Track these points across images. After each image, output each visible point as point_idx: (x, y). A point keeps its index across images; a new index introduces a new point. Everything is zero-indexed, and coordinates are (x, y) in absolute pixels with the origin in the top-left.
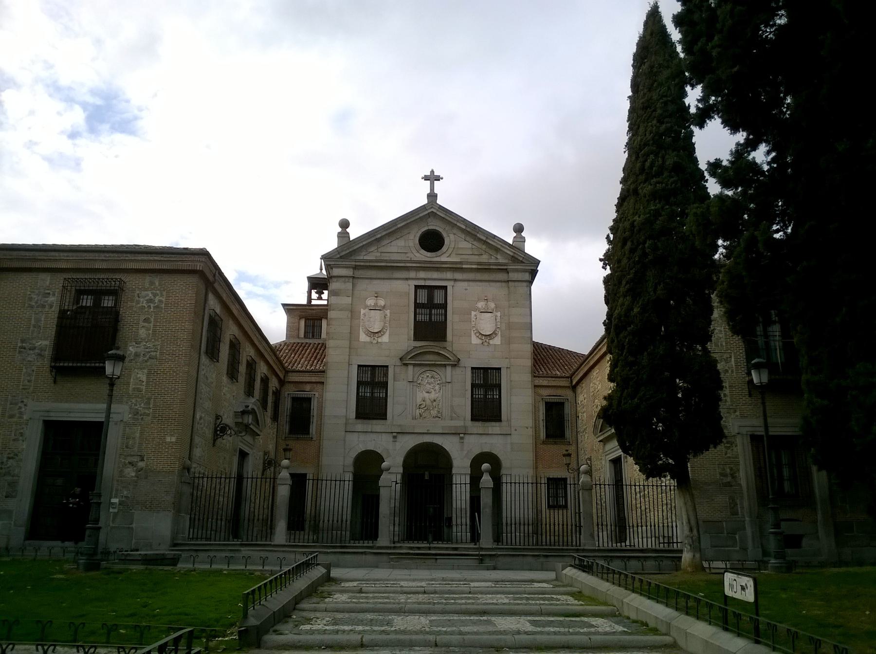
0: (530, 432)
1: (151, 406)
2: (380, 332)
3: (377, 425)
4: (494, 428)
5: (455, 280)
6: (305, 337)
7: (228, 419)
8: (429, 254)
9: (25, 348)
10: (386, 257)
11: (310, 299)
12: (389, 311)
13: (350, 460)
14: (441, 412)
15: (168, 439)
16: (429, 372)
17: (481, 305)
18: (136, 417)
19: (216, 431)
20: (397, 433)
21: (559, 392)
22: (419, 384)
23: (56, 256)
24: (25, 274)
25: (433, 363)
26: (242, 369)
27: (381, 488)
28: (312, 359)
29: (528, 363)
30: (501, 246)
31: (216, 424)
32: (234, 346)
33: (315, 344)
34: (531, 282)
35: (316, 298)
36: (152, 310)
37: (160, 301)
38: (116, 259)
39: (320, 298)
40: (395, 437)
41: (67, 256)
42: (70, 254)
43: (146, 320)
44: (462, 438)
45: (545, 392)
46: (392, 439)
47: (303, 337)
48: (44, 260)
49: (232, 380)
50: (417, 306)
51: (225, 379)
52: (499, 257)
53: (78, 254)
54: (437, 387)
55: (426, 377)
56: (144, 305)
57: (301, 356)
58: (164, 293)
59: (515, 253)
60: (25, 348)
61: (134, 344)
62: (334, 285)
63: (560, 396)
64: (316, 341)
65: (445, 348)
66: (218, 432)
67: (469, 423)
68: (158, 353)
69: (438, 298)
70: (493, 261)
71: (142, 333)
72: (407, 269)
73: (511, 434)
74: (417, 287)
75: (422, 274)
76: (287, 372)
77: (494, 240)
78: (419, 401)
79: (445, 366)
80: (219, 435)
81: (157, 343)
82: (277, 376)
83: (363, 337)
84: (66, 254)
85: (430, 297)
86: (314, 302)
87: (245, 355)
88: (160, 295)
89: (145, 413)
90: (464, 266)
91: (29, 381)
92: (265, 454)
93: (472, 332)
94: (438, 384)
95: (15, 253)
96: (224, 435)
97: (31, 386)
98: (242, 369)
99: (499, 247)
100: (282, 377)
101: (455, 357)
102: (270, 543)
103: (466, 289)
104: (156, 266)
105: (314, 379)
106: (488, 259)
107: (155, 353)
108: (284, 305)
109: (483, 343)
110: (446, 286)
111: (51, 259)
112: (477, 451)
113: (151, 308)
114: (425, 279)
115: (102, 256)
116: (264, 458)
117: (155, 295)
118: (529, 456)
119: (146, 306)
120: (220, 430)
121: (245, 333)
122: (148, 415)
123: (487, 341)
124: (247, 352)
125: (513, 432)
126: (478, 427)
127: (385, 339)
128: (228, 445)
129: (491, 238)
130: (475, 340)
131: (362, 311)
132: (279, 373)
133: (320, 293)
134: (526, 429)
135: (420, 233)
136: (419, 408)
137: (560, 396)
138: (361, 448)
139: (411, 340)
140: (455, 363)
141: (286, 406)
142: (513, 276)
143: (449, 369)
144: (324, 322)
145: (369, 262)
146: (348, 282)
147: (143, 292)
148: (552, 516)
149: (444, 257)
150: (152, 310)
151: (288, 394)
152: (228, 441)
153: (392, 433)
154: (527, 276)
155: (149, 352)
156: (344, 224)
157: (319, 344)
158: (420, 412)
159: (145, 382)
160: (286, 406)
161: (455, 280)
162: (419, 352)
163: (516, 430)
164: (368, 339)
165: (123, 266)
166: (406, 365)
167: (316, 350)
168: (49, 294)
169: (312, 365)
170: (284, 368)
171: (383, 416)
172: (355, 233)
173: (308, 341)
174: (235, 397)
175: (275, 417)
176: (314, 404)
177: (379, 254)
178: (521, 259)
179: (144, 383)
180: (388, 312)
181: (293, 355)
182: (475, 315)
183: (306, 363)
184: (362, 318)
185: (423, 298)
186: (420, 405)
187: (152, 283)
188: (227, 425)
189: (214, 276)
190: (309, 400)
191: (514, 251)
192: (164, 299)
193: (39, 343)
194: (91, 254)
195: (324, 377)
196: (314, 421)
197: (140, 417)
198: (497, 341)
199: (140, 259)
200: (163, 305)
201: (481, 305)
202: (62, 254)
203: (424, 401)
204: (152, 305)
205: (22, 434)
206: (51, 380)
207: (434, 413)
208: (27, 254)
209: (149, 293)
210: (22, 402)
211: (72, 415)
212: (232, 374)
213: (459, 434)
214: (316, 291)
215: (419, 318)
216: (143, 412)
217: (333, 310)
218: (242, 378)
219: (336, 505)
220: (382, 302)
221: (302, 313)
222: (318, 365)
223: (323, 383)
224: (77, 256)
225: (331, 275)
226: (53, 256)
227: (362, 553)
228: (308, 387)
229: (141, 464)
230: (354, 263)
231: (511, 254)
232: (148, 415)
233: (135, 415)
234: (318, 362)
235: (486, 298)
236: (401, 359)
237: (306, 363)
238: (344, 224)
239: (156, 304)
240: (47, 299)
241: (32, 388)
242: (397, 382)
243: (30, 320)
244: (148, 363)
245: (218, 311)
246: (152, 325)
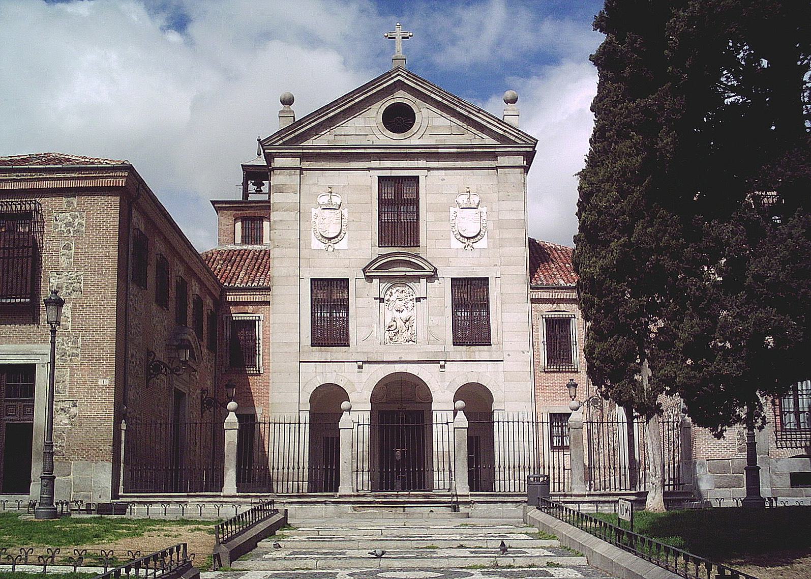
0: (527, 357)
1: (80, 345)
2: (336, 237)
3: (337, 353)
4: (480, 352)
5: (429, 169)
6: (245, 240)
7: (161, 355)
8: (396, 136)
10: (342, 141)
11: (246, 193)
12: (346, 209)
13: (306, 397)
15: (101, 382)
16: (399, 285)
17: (463, 199)
18: (64, 358)
19: (148, 369)
20: (364, 362)
21: (563, 306)
25: (404, 274)
26: (172, 293)
27: (341, 430)
28: (254, 273)
29: (523, 269)
30: (488, 122)
31: (148, 361)
32: (163, 268)
33: (256, 251)
34: (526, 169)
35: (254, 191)
36: (72, 234)
37: (80, 224)
39: (259, 192)
40: (360, 367)
43: (65, 247)
44: (443, 367)
45: (545, 307)
46: (357, 370)
47: (240, 242)
49: (162, 308)
50: (381, 202)
51: (154, 307)
52: (484, 136)
54: (410, 304)
56: (62, 229)
57: (239, 268)
58: (84, 215)
59: (505, 131)
61: (55, 275)
62: (277, 179)
63: (564, 311)
64: (257, 247)
65: (417, 256)
66: (152, 371)
67: (451, 347)
68: (82, 284)
69: (408, 194)
70: (477, 142)
71: (64, 262)
72: (368, 157)
73: (503, 361)
74: (380, 179)
75: (388, 163)
76: (225, 291)
77: (479, 115)
78: (388, 321)
79: (417, 278)
80: (152, 374)
81: (79, 273)
82: (211, 294)
83: (317, 244)
85: (399, 193)
86: (251, 198)
87: (173, 274)
88: (79, 217)
89: (73, 353)
90: (440, 150)
92: (203, 392)
93: (451, 232)
94: (411, 300)
96: (158, 374)
98: (172, 293)
99: (485, 123)
100: (217, 296)
102: (218, 493)
103: (443, 180)
104: (73, 184)
105: (257, 298)
106: (471, 140)
107: (79, 284)
108: (213, 203)
109: (465, 248)
110: (418, 176)
112: (461, 382)
113: (70, 233)
114: (391, 169)
116: (202, 397)
117: (74, 218)
118: (526, 387)
119: (65, 231)
120: (153, 369)
121: (172, 249)
122: (77, 355)
123: (471, 244)
124: (178, 270)
125: (506, 358)
126: (463, 352)
127: (343, 245)
128: (162, 385)
129: (474, 112)
130: (456, 244)
131: (314, 211)
132: (213, 291)
133: (259, 185)
134: (522, 353)
135: (384, 108)
136: (389, 330)
137: (564, 311)
138: (320, 381)
140: (431, 273)
141: (225, 334)
142: (503, 161)
143: (423, 281)
144: (266, 224)
145: (320, 149)
146: (294, 174)
147: (60, 214)
148: (551, 457)
149: (414, 139)
150: (72, 234)
151: (227, 317)
152: (161, 380)
153: (357, 362)
154: (520, 161)
155: (72, 283)
156: (288, 101)
157: (261, 251)
159: (70, 318)
160: (225, 334)
161: (429, 169)
163: (509, 355)
164: (323, 246)
165: (37, 185)
166: (370, 279)
167: (257, 259)
169: (253, 281)
170: (220, 285)
171: (344, 342)
172: (300, 111)
173: (245, 247)
174: (166, 327)
175: (212, 347)
176: (259, 330)
177: (332, 138)
178: (513, 138)
179: (70, 319)
180: (345, 212)
181: (229, 267)
182: (455, 212)
183: (247, 277)
184: (313, 220)
185: (389, 194)
186: (389, 327)
187: (69, 204)
188: (159, 362)
189: (138, 189)
190: (251, 324)
191: (505, 129)
192: (84, 222)
195: (269, 295)
196: (261, 349)
197: (68, 358)
198: (482, 244)
199: (55, 177)
200: (84, 229)
201: (463, 199)
204: (72, 229)
207: (407, 335)
209: (68, 215)
212: (162, 300)
213: (438, 362)
214: (253, 181)
215: (385, 217)
216: (71, 352)
217: (277, 211)
218: (172, 305)
219: (292, 450)
220: (336, 200)
221: (237, 212)
222: (262, 280)
223: (268, 303)
225: (273, 166)
227: (321, 503)
228: (250, 308)
229: (74, 410)
230: (301, 151)
231: (501, 132)
232: (77, 355)
233: (63, 356)
234: (261, 276)
235: (468, 190)
236: (364, 270)
237: (247, 277)
238: (288, 101)
239: (76, 228)
244: (73, 297)
245: (142, 230)
246: (73, 251)
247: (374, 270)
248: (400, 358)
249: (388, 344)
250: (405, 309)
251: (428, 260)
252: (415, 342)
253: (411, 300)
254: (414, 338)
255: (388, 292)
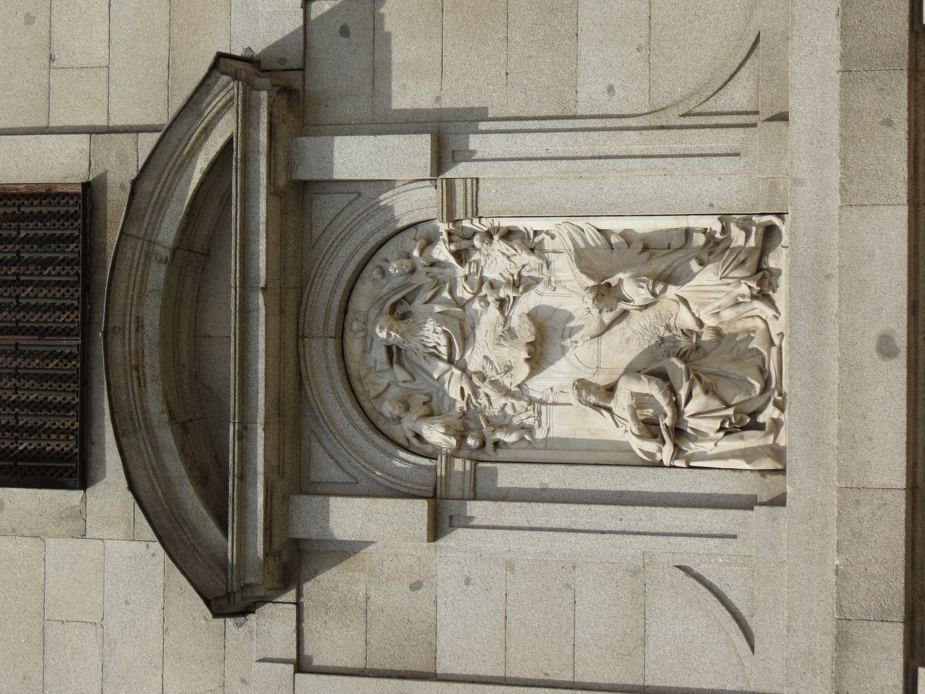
14: (715, 225)
16: (354, 346)
22: (462, 437)
55: (400, 374)
101: (215, 101)
136: (678, 433)
139: (81, 514)
158: (709, 426)
162: (167, 437)
186: (650, 429)
203: (611, 390)
242: (442, 643)
247: (223, 524)
248: (885, 348)
249: (782, 441)
250: (529, 301)
251: (164, 120)
252: (770, 233)
253: (461, 256)
254: (738, 237)
255: (409, 424)
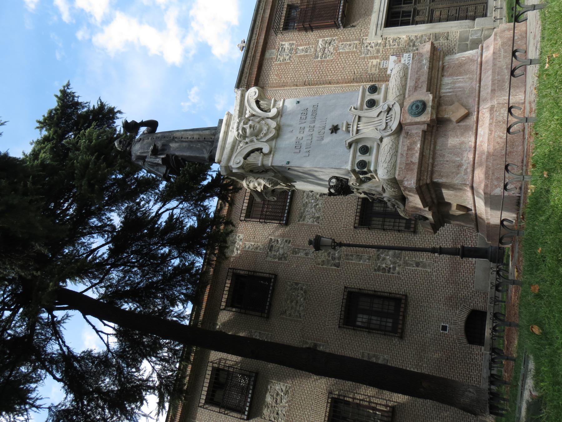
9: (323, 55)
23: (254, 42)
24: (263, 68)
38: (264, 3)
41: (256, 34)
42: (255, 32)
48: (255, 52)
53: (256, 27)
60: (323, 55)
84: (254, 35)
91: (350, 45)
95: (246, 70)
97: (354, 44)
111: (256, 45)
115: (261, 11)
168: (282, 48)
193: (320, 46)
194: (258, 19)
202: (253, 38)
205: (394, 40)
206: (353, 29)
208: (248, 61)
210: (367, 46)
211: (382, 9)
224: (258, 28)
226: (254, 44)
240: (286, 49)
241: (356, 42)
243: (300, 56)
